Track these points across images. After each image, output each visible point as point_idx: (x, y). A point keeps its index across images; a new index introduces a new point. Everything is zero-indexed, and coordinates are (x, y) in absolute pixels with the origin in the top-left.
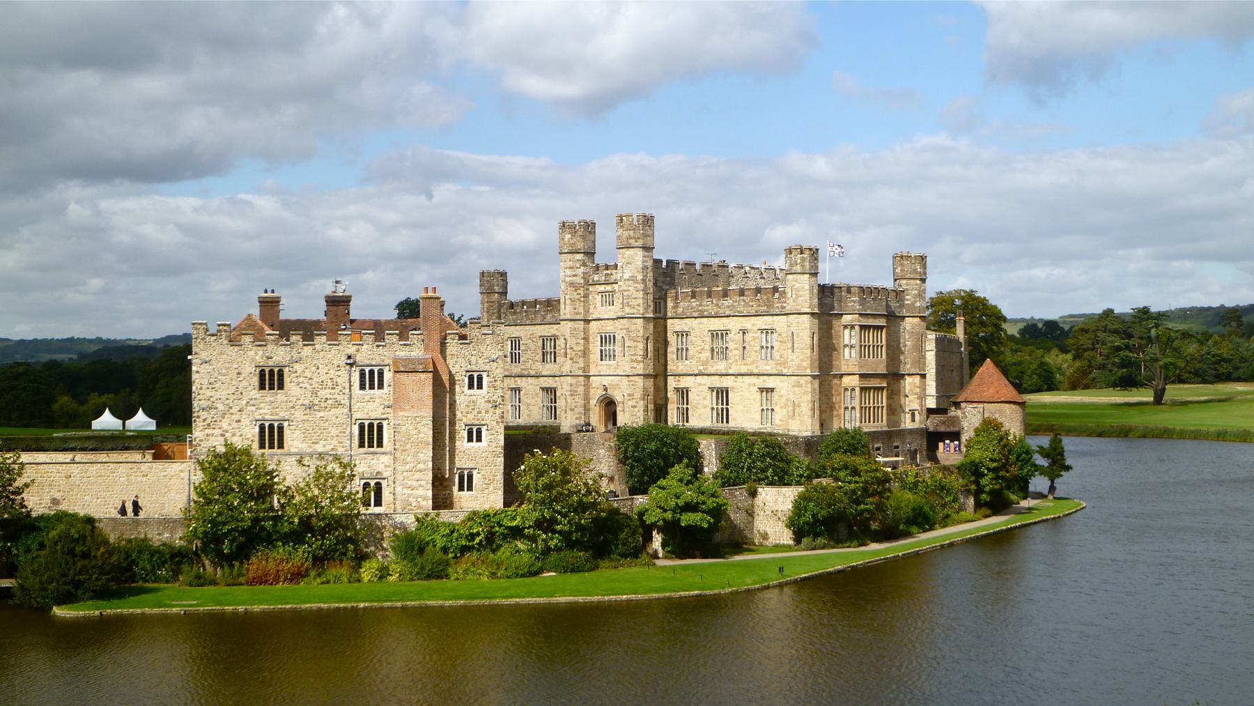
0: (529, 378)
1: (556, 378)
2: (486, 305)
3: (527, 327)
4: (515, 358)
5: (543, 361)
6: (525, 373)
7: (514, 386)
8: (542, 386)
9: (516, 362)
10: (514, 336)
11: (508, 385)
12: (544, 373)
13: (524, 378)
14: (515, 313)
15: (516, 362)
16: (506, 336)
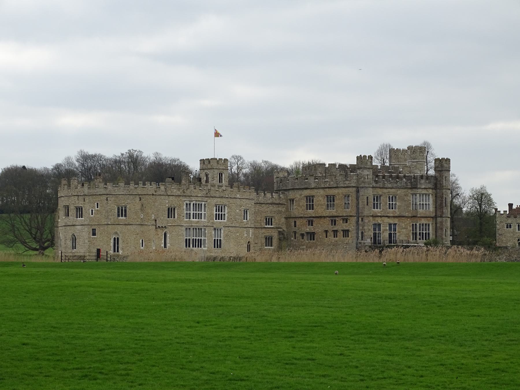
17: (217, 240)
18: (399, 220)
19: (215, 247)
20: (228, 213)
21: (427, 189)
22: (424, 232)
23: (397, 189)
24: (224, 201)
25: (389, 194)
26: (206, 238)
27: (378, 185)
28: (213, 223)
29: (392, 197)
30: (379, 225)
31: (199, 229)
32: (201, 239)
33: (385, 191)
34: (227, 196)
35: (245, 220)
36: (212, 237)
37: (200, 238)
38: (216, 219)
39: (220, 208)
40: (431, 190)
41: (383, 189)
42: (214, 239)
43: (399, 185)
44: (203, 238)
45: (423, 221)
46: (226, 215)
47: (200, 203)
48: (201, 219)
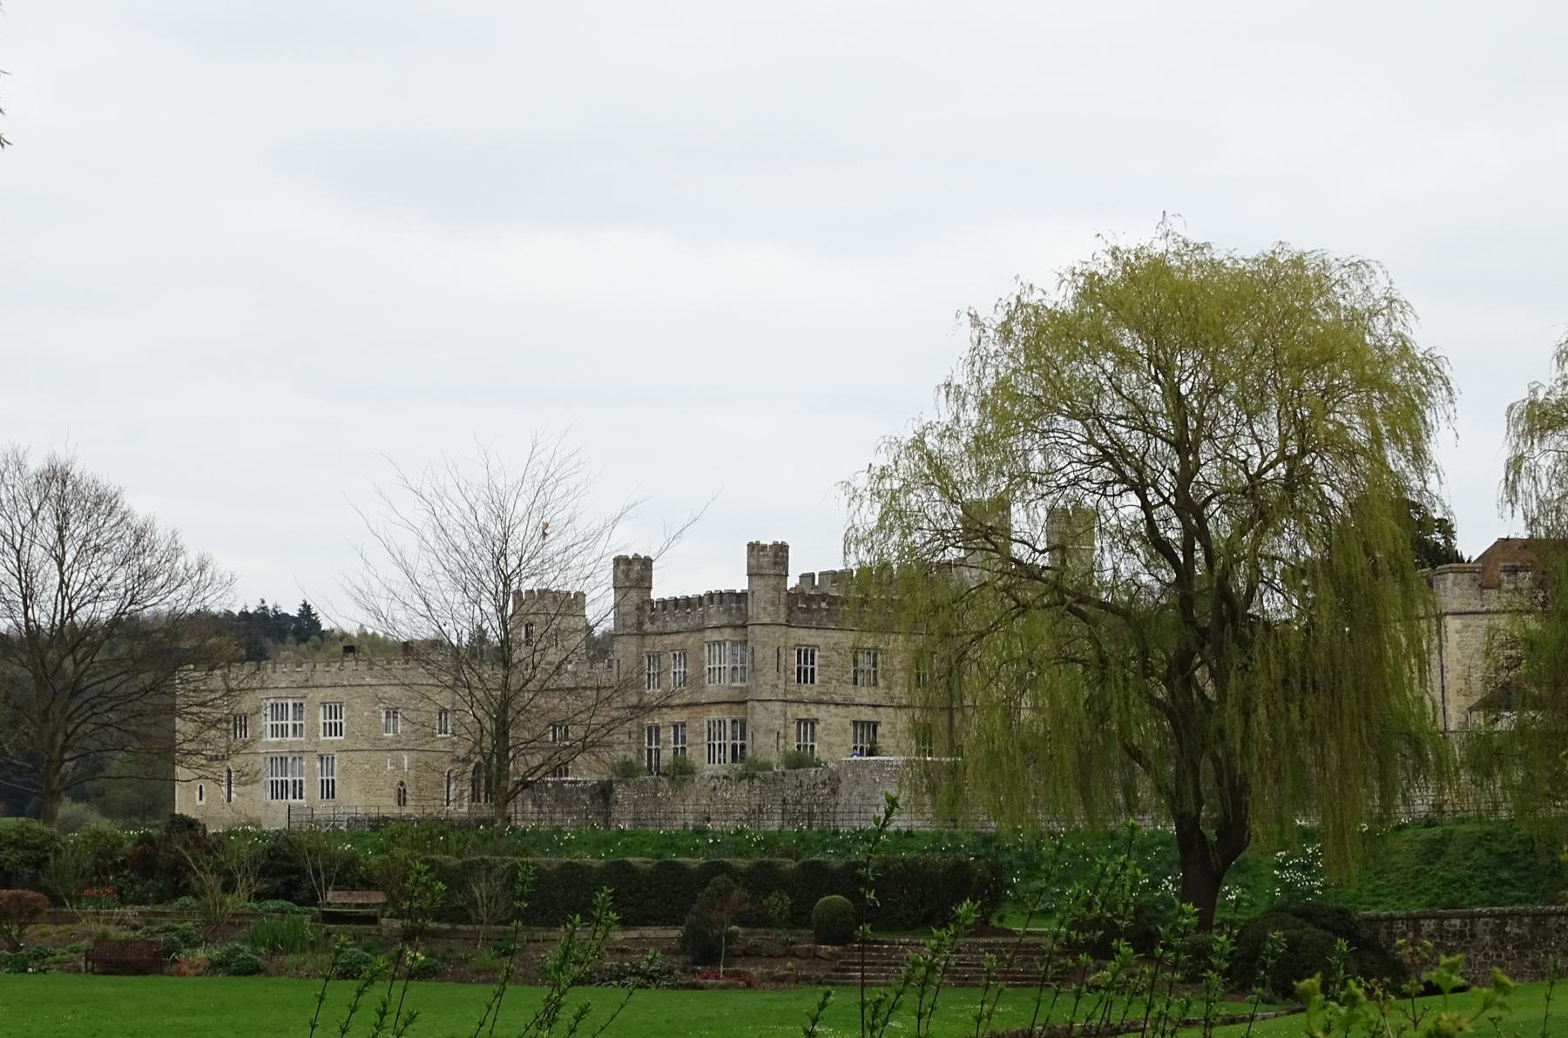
0: (832, 706)
1: (881, 709)
2: (783, 594)
3: (829, 633)
4: (805, 676)
5: (855, 683)
6: (825, 698)
7: (805, 717)
8: (856, 718)
9: (806, 682)
10: (805, 643)
11: (792, 715)
12: (857, 700)
13: (823, 707)
14: (808, 610)
15: (806, 682)
16: (792, 643)
17: (328, 781)
18: (691, 713)
19: (322, 797)
20: (348, 719)
21: (722, 630)
22: (717, 743)
23: (687, 634)
24: (340, 694)
25: (673, 648)
26: (303, 779)
27: (654, 629)
28: (317, 744)
29: (680, 655)
30: (658, 729)
31: (282, 758)
32: (287, 781)
33: (667, 640)
34: (345, 683)
35: (391, 735)
36: (315, 776)
37: (284, 779)
38: (325, 735)
39: (333, 709)
40: (728, 631)
41: (664, 637)
42: (319, 779)
43: (692, 623)
44: (290, 779)
45: (715, 714)
46: (344, 725)
47: (284, 702)
48: (287, 736)
